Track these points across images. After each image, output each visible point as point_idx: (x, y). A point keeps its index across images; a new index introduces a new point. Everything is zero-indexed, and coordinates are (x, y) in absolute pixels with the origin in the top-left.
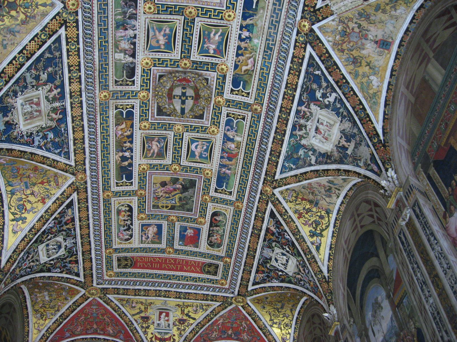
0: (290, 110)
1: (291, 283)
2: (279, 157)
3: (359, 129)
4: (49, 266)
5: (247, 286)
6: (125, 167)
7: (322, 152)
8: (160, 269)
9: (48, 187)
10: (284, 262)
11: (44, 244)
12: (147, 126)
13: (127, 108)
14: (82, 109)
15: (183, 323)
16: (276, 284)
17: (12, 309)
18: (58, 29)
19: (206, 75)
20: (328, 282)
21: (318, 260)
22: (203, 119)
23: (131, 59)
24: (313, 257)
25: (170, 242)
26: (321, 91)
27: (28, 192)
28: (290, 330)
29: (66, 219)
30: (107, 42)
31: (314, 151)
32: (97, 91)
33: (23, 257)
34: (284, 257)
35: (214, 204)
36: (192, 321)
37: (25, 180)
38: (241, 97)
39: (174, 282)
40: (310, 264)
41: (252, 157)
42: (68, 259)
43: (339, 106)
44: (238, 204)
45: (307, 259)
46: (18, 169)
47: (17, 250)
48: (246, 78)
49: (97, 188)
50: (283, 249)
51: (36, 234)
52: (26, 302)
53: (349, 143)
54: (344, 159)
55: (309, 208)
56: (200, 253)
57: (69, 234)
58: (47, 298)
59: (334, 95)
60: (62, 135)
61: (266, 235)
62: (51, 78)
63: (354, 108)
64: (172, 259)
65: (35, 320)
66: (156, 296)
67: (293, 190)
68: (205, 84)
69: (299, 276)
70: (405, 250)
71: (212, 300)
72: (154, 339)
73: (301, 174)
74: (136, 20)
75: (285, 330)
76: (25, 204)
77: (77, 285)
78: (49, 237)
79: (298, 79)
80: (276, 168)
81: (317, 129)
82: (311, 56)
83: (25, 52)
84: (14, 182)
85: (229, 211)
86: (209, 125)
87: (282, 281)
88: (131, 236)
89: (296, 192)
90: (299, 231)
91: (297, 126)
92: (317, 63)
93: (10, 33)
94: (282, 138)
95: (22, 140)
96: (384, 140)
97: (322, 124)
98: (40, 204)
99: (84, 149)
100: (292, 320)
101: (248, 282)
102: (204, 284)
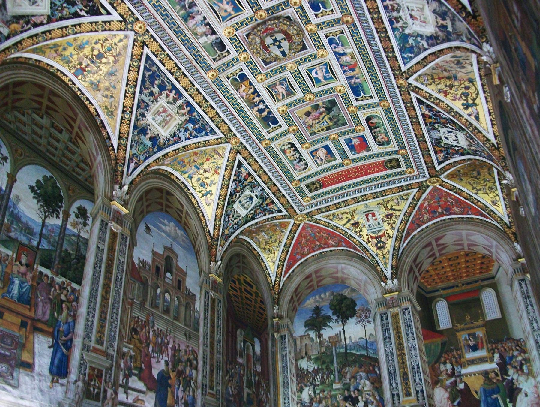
0: (378, 8)
1: (471, 155)
3: (446, 6)
4: (251, 216)
5: (434, 167)
6: (266, 116)
7: (429, 35)
8: (348, 179)
9: (214, 161)
10: (455, 138)
11: (237, 203)
12: (263, 77)
13: (237, 74)
14: (201, 94)
15: (391, 217)
16: (458, 158)
17: (241, 257)
18: (142, 51)
19: (285, 14)
20: (498, 149)
21: (481, 129)
22: (307, 49)
23: (214, 37)
24: (476, 128)
25: (344, 155)
27: (201, 171)
28: (497, 192)
29: (243, 176)
30: (186, 35)
31: (421, 36)
32: (204, 75)
33: (224, 220)
34: (452, 134)
35: (363, 111)
36: (398, 213)
37: (194, 164)
38: (327, 16)
39: (365, 186)
40: (475, 135)
41: (371, 60)
42: (264, 204)
44: (384, 103)
45: (470, 131)
46: (183, 161)
47: (217, 218)
49: (254, 142)
50: (447, 127)
51: (225, 199)
52: (251, 245)
53: (445, 21)
54: (450, 37)
55: (450, 85)
56: (375, 154)
57: (252, 186)
58: (266, 237)
60: (199, 121)
61: (425, 120)
62: (162, 88)
64: (354, 168)
65: (266, 256)
66: (356, 203)
67: (426, 74)
68: (288, 23)
69: (472, 148)
71: (409, 189)
72: (370, 239)
73: (423, 60)
74: (197, 6)
75: (492, 193)
76: (205, 180)
77: (284, 219)
78: (238, 196)
80: (398, 62)
81: (411, 16)
83: (130, 83)
84: (186, 170)
85: (379, 112)
86: (316, 51)
87: (462, 154)
88: (306, 164)
89: (428, 75)
90: (451, 108)
91: (393, 20)
93: (111, 75)
94: (386, 35)
95: (170, 142)
96: (473, 10)
97: (413, 10)
98: (216, 176)
99: (223, 121)
100: (495, 182)
101: (433, 163)
102: (394, 178)
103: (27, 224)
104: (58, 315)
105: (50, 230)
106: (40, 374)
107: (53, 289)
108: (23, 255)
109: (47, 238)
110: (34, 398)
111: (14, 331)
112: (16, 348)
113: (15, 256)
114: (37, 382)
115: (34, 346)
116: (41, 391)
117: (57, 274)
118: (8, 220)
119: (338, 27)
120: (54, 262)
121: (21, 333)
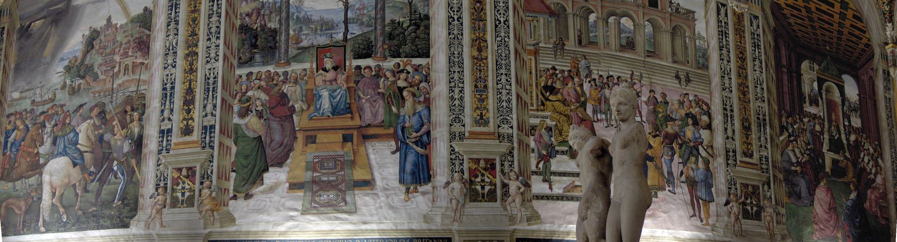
103: (322, 19)
104: (398, 110)
105: (359, 9)
106: (385, 189)
107: (382, 79)
108: (326, 60)
109: (355, 21)
110: (382, 218)
111: (336, 151)
112: (342, 169)
113: (315, 66)
114: (383, 199)
115: (368, 159)
116: (391, 207)
117: (385, 58)
118: (294, 31)
120: (376, 45)
121: (345, 149)
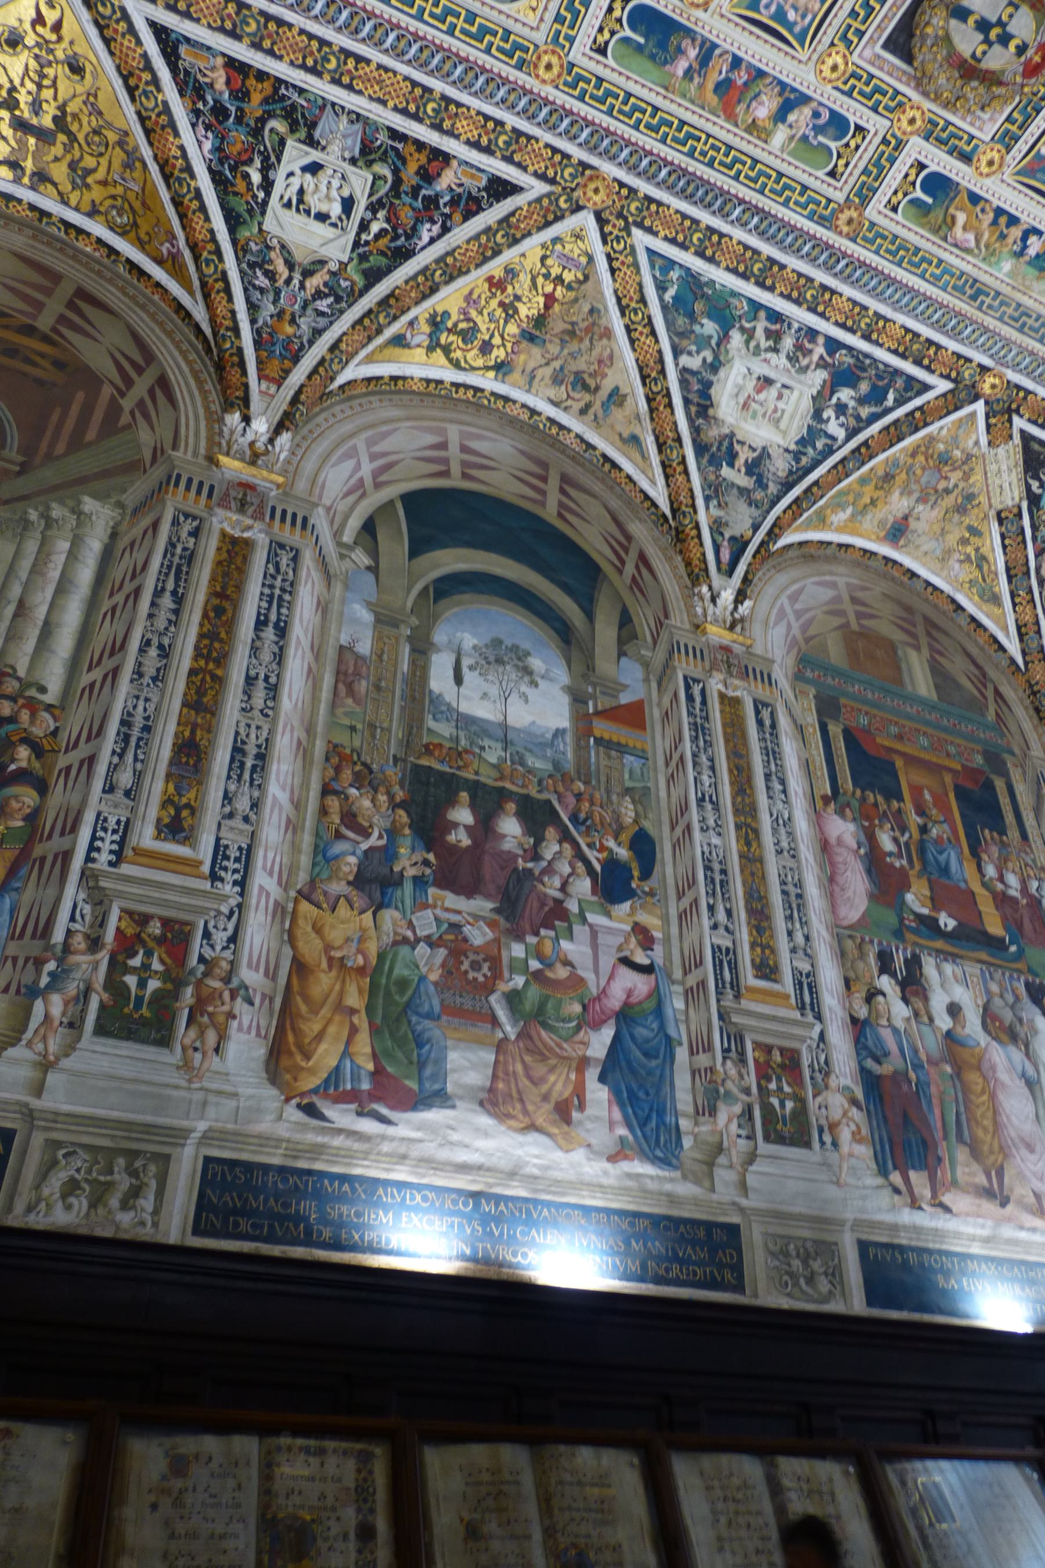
0: (822, 315)
2: (700, 254)
21: (371, 347)
26: (852, 404)
31: (714, 367)
34: (336, 210)
43: (819, 445)
48: (938, 215)
50: (373, 208)
59: (841, 434)
61: (420, 145)
63: (816, 483)
70: (690, 714)
79: (889, 349)
81: (766, 382)
82: (926, 388)
92: (910, 399)
97: (780, 397)
119: (852, 181)
